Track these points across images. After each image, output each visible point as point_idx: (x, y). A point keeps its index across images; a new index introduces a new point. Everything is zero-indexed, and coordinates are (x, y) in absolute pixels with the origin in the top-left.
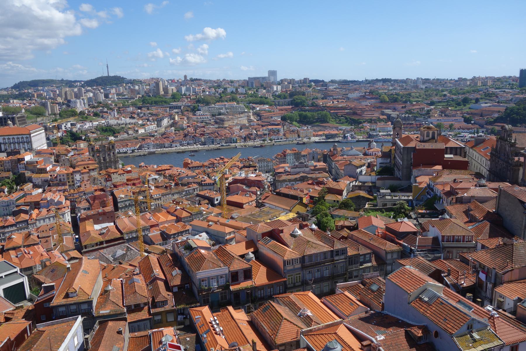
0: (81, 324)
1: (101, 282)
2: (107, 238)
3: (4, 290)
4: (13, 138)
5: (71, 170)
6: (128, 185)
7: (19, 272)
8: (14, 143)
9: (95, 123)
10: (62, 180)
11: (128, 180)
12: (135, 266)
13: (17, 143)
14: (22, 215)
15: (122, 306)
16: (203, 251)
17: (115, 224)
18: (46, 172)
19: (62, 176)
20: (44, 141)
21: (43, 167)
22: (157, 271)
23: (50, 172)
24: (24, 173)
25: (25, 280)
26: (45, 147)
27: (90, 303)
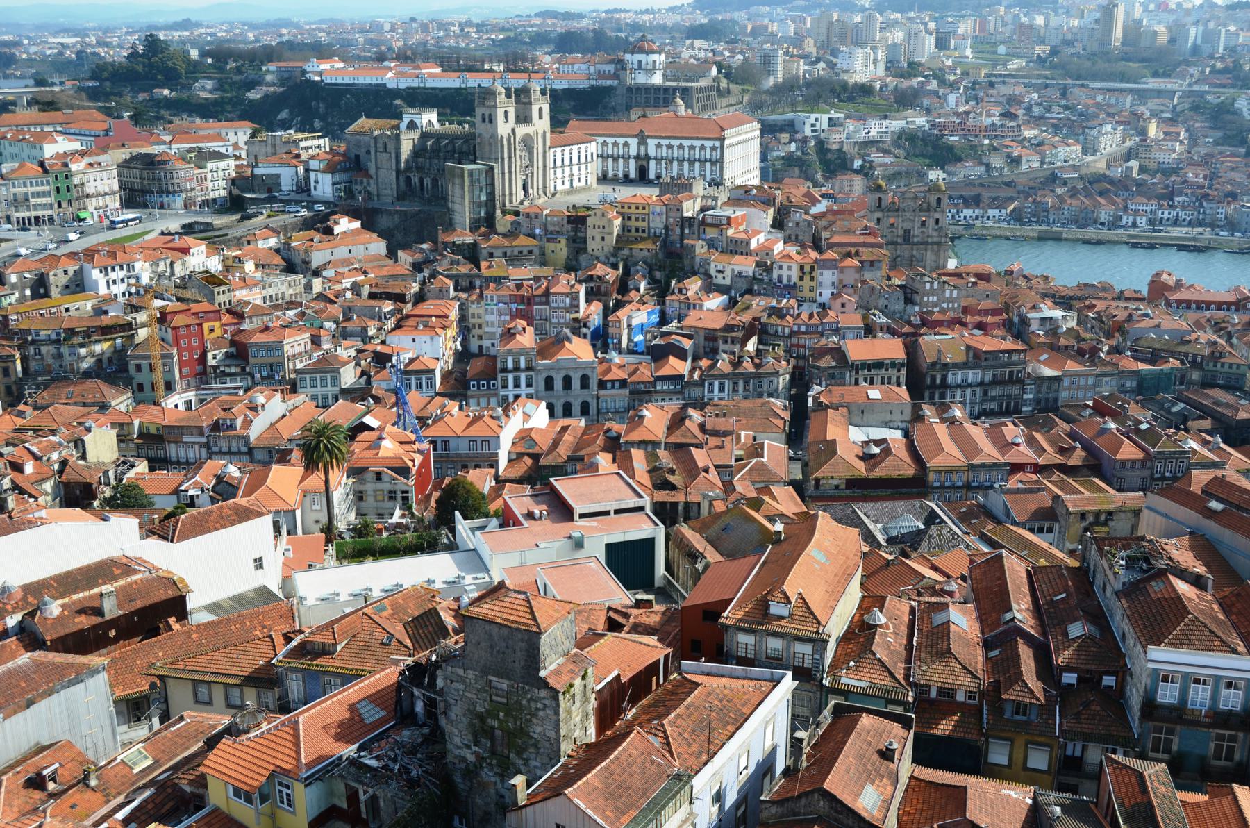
0: (789, 696)
1: (853, 595)
2: (878, 472)
3: (609, 547)
4: (681, 147)
5: (814, 255)
6: (964, 325)
7: (648, 510)
8: (681, 161)
9: (896, 125)
10: (785, 281)
11: (965, 310)
12: (948, 576)
13: (689, 160)
14: (673, 360)
15: (903, 682)
16: (1182, 587)
17: (907, 434)
18: (749, 254)
19: (785, 267)
20: (755, 162)
21: (743, 236)
22: (1021, 612)
25: (660, 533)
26: (754, 179)
27: (819, 643)
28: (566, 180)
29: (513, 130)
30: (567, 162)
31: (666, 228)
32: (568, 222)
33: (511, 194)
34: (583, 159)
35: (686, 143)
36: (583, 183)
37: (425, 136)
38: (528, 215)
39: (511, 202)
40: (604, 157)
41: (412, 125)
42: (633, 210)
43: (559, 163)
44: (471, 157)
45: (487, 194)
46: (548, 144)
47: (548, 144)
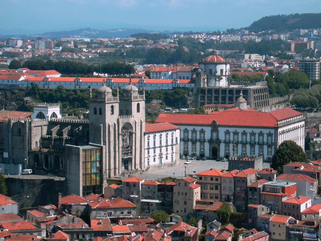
4: (244, 133)
8: (244, 144)
21: (295, 202)
23: (305, 213)
24: (255, 209)
28: (157, 157)
29: (118, 120)
30: (158, 144)
31: (234, 195)
32: (159, 190)
33: (115, 168)
34: (170, 143)
35: (248, 131)
36: (169, 160)
37: (52, 124)
38: (128, 184)
39: (115, 174)
40: (185, 140)
41: (41, 116)
42: (209, 181)
43: (151, 145)
44: (85, 140)
45: (97, 168)
46: (144, 131)
47: (144, 131)
